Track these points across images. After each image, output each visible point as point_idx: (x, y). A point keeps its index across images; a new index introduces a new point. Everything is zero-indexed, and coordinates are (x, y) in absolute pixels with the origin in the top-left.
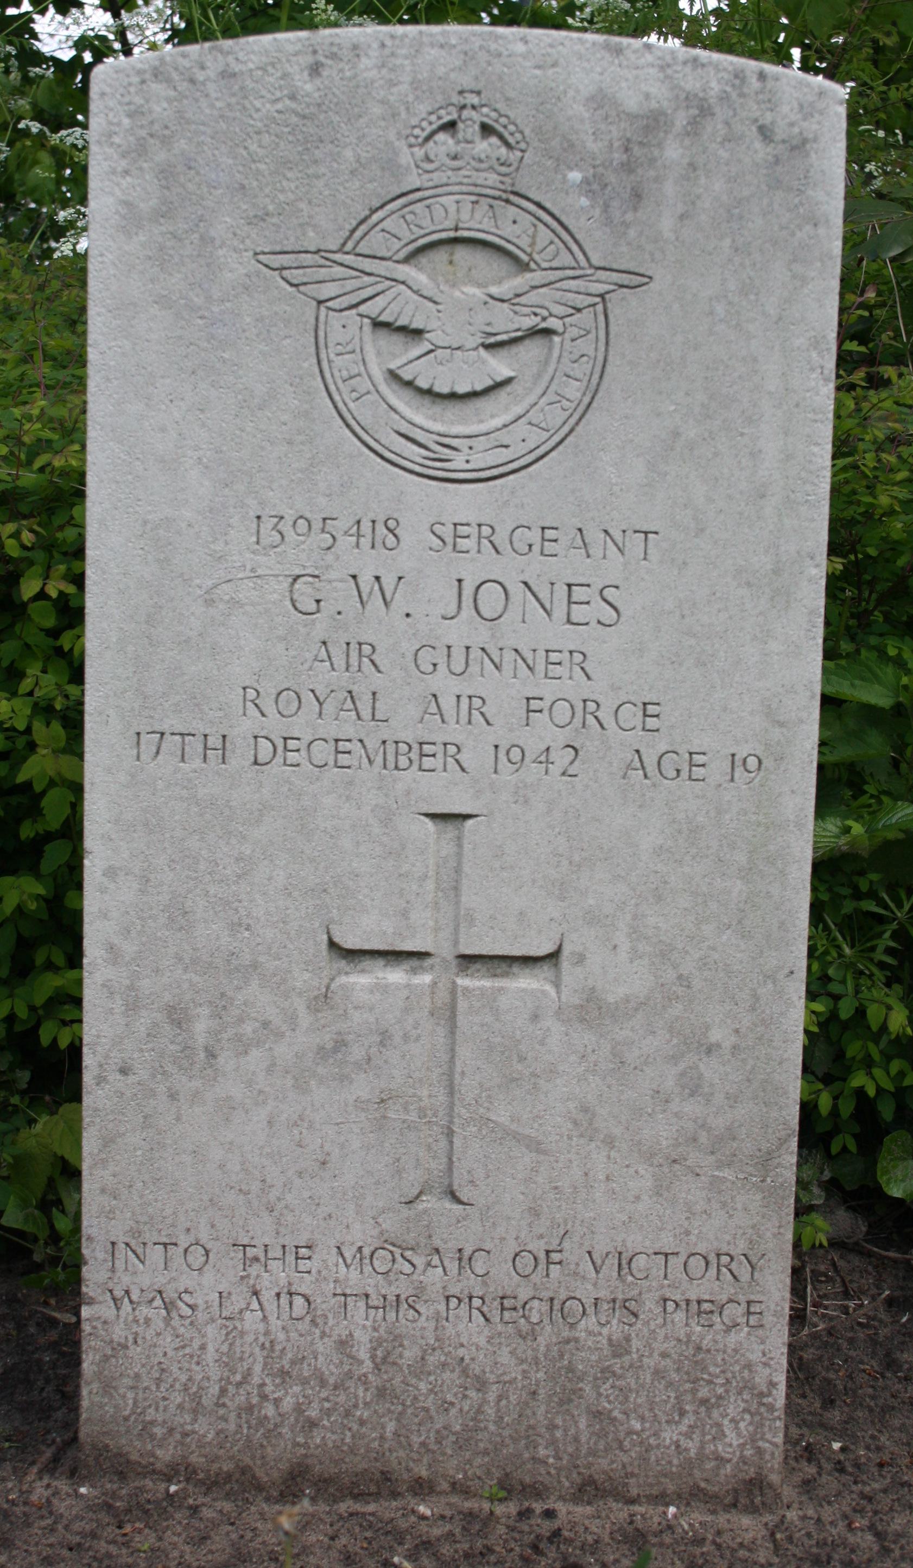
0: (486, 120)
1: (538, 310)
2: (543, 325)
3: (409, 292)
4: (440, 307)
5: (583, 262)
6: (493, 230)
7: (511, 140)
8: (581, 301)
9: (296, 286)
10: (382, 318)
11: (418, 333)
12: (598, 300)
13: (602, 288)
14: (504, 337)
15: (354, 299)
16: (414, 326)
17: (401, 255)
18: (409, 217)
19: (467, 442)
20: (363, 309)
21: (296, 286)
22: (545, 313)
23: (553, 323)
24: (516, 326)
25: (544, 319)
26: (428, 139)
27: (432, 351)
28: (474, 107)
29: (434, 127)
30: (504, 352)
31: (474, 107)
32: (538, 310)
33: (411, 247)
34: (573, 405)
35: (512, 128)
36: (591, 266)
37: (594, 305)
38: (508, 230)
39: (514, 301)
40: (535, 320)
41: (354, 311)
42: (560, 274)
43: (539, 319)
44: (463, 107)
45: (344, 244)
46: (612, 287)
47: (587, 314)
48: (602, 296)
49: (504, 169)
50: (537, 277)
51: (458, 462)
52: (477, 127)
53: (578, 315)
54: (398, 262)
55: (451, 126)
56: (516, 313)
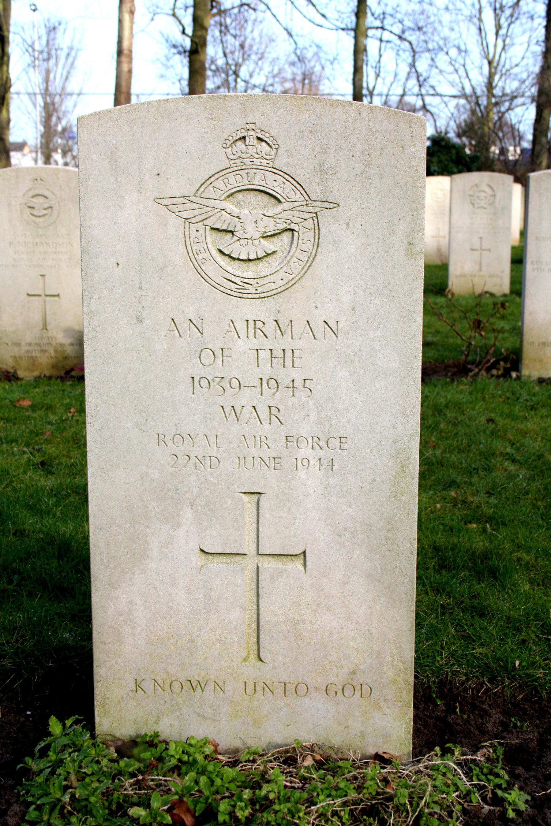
0: (260, 136)
1: (287, 221)
2: (289, 227)
5: (307, 198)
7: (271, 143)
8: (306, 216)
11: (232, 232)
12: (314, 215)
13: (316, 210)
17: (223, 197)
19: (256, 281)
20: (206, 222)
22: (289, 222)
23: (292, 226)
29: (234, 139)
30: (271, 239)
32: (287, 221)
38: (271, 184)
39: (276, 216)
42: (297, 204)
48: (316, 213)
49: (268, 157)
50: (286, 206)
51: (252, 290)
52: (255, 137)
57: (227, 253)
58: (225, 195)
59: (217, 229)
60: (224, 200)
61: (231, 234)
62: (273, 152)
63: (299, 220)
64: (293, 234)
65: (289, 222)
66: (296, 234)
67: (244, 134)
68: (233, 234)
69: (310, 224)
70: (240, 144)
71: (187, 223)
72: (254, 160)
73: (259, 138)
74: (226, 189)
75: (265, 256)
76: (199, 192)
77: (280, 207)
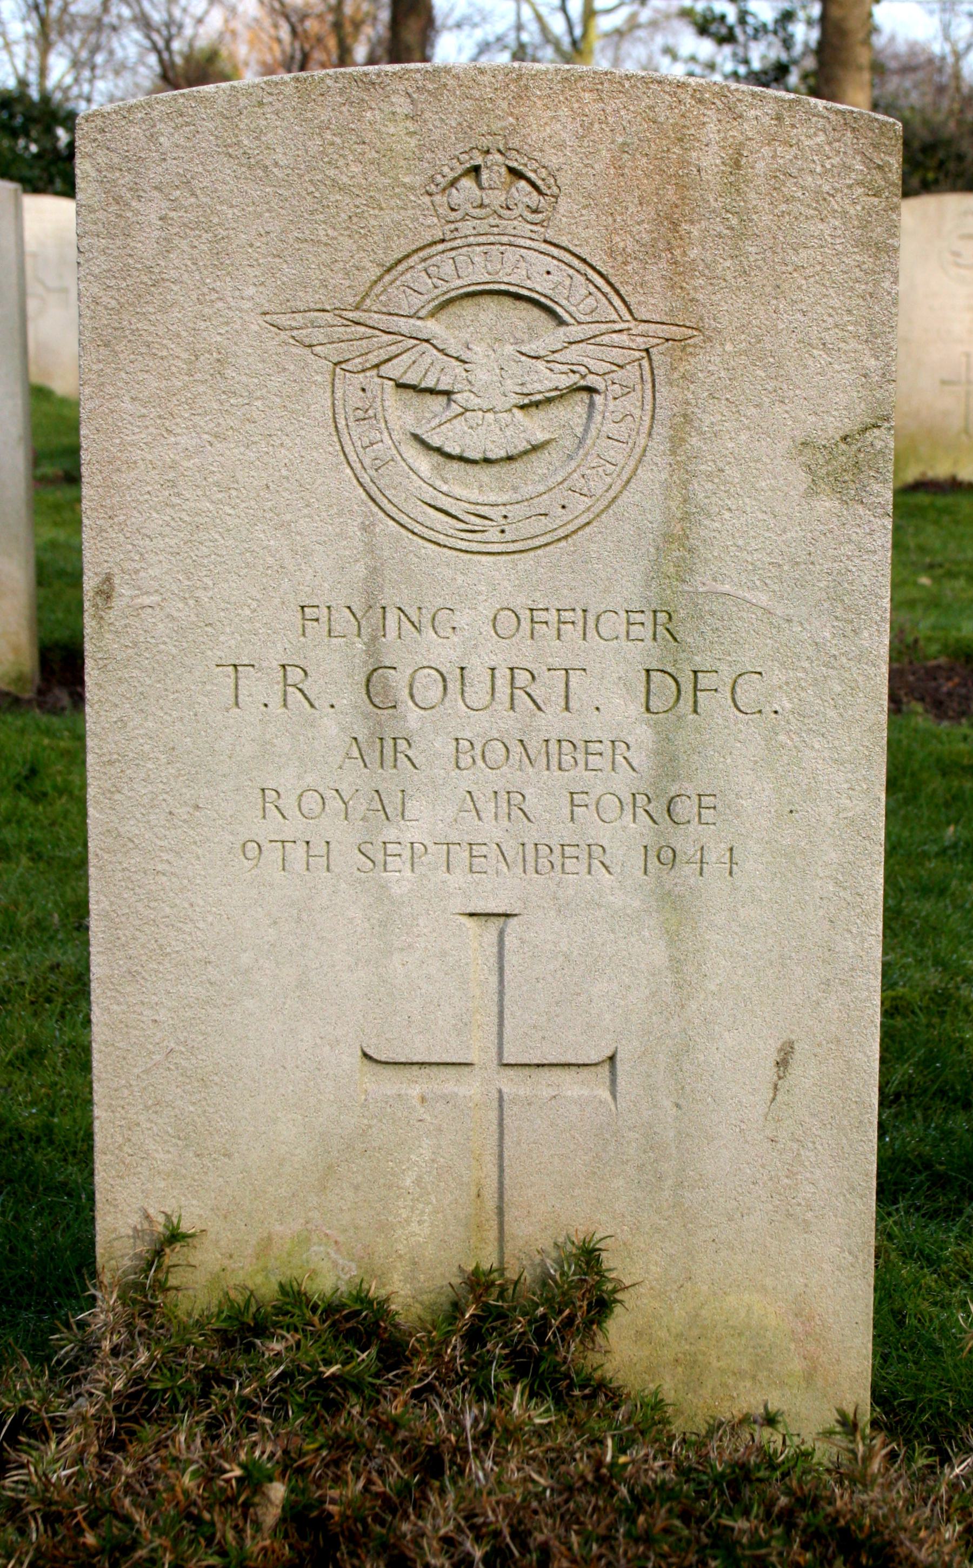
2: (583, 383)
3: (435, 352)
4: (467, 366)
9: (310, 346)
12: (644, 354)
14: (539, 397)
15: (373, 359)
16: (442, 387)
18: (432, 270)
20: (384, 370)
21: (310, 346)
22: (582, 369)
23: (591, 380)
24: (552, 386)
25: (583, 377)
27: (462, 414)
31: (499, 151)
32: (575, 368)
34: (618, 469)
35: (544, 173)
36: (635, 319)
40: (575, 378)
41: (374, 372)
43: (577, 376)
47: (633, 369)
48: (647, 350)
50: (575, 332)
52: (503, 170)
53: (621, 373)
54: (419, 318)
56: (551, 370)
57: (435, 441)
59: (413, 388)
61: (442, 399)
64: (591, 398)
65: (582, 369)
67: (479, 161)
68: (449, 400)
69: (631, 374)
70: (467, 183)
72: (497, 221)
75: (526, 452)
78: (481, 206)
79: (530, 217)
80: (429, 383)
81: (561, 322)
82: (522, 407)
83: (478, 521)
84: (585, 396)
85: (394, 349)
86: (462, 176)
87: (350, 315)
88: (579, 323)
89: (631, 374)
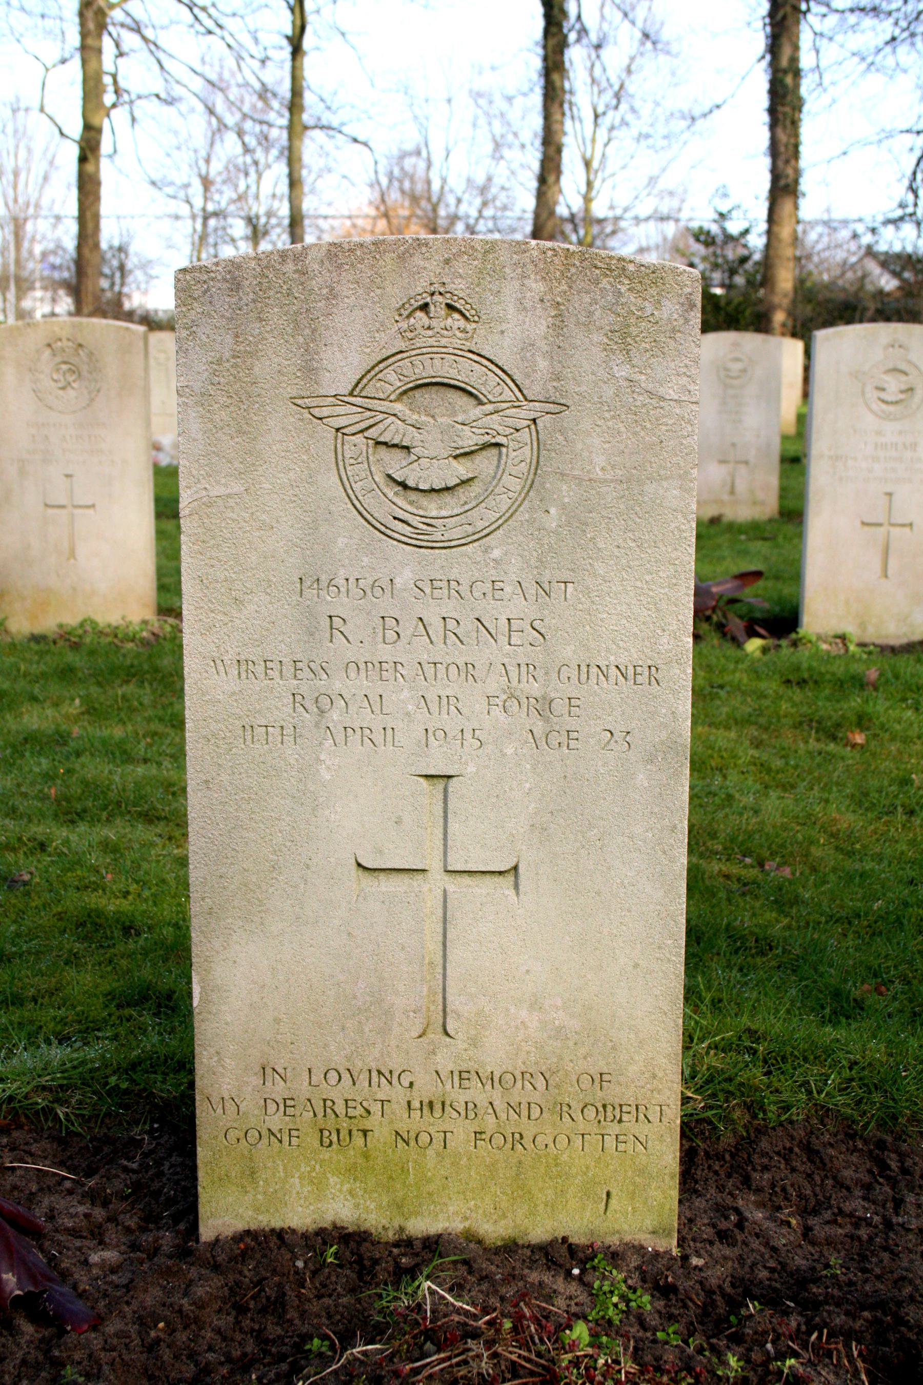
0: (449, 301)
2: (493, 441)
6: (459, 378)
7: (468, 314)
9: (320, 419)
10: (382, 439)
13: (532, 415)
14: (467, 450)
20: (366, 434)
21: (320, 419)
23: (499, 439)
26: (408, 317)
28: (440, 294)
31: (440, 294)
33: (401, 390)
36: (526, 400)
37: (528, 426)
39: (474, 424)
40: (487, 438)
41: (360, 435)
42: (505, 405)
44: (432, 294)
45: (353, 390)
46: (540, 414)
48: (534, 420)
50: (489, 408)
52: (443, 306)
53: (518, 434)
55: (425, 307)
58: (398, 392)
59: (385, 444)
60: (395, 401)
62: (470, 327)
63: (508, 431)
66: (504, 450)
67: (428, 300)
71: (340, 435)
73: (449, 306)
74: (399, 384)
75: (457, 485)
76: (358, 389)
77: (478, 411)
78: (429, 328)
79: (459, 334)
80: (395, 441)
81: (481, 403)
82: (456, 457)
83: (425, 527)
84: (494, 451)
85: (371, 422)
86: (416, 309)
87: (345, 399)
88: (490, 402)
89: (525, 435)
